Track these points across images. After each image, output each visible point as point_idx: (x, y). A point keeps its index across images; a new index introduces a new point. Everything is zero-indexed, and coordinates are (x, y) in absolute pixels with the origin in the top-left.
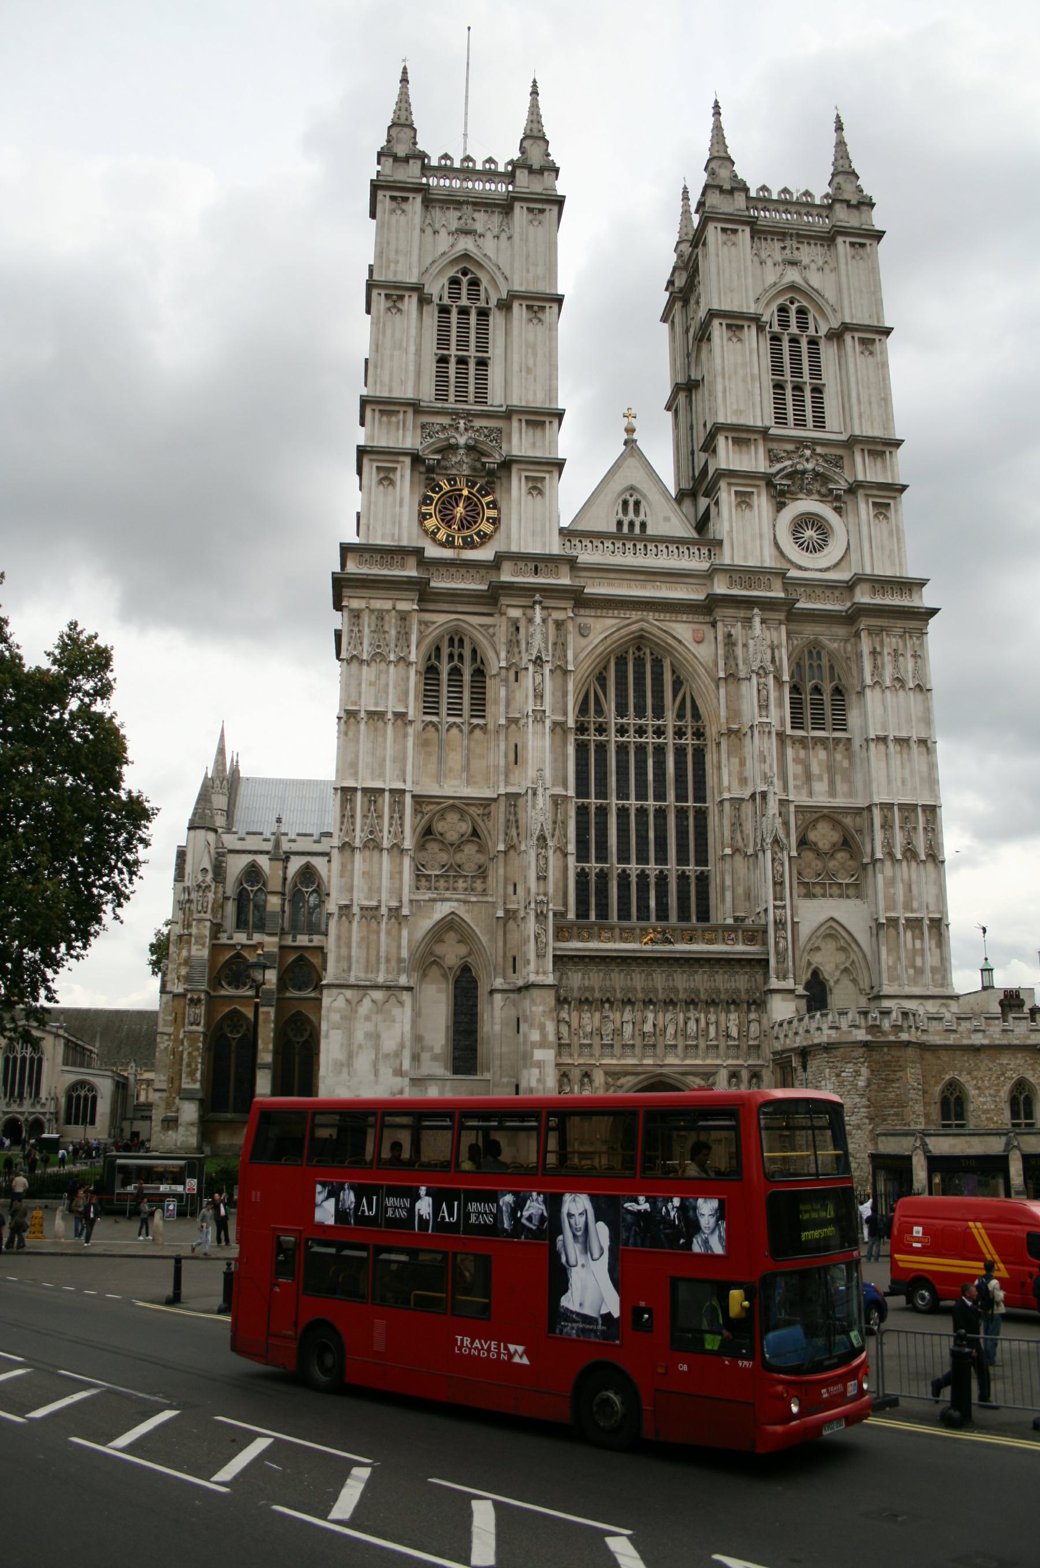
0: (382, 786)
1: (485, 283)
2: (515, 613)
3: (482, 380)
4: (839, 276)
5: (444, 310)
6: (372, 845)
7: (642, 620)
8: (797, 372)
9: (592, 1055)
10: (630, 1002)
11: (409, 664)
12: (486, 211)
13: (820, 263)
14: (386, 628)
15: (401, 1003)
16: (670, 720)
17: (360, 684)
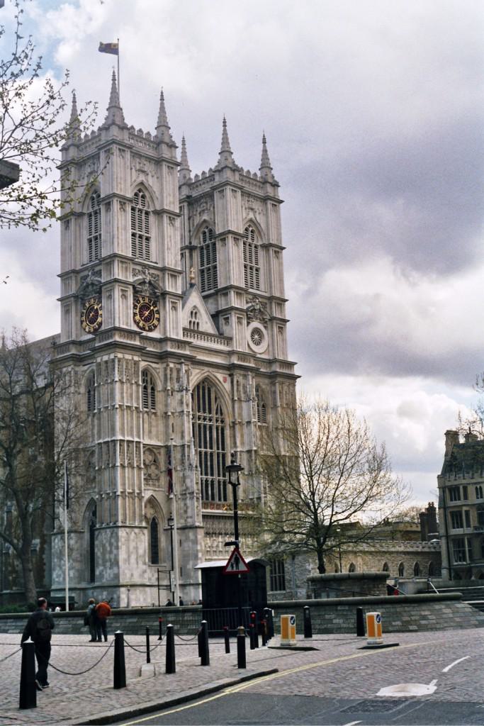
0: (131, 439)
1: (148, 199)
2: (172, 365)
3: (148, 246)
4: (267, 217)
5: (133, 209)
6: (131, 466)
7: (208, 371)
8: (251, 262)
9: (210, 555)
10: (220, 534)
11: (138, 385)
12: (150, 162)
13: (260, 209)
14: (129, 368)
15: (144, 534)
16: (214, 415)
17: (122, 393)
